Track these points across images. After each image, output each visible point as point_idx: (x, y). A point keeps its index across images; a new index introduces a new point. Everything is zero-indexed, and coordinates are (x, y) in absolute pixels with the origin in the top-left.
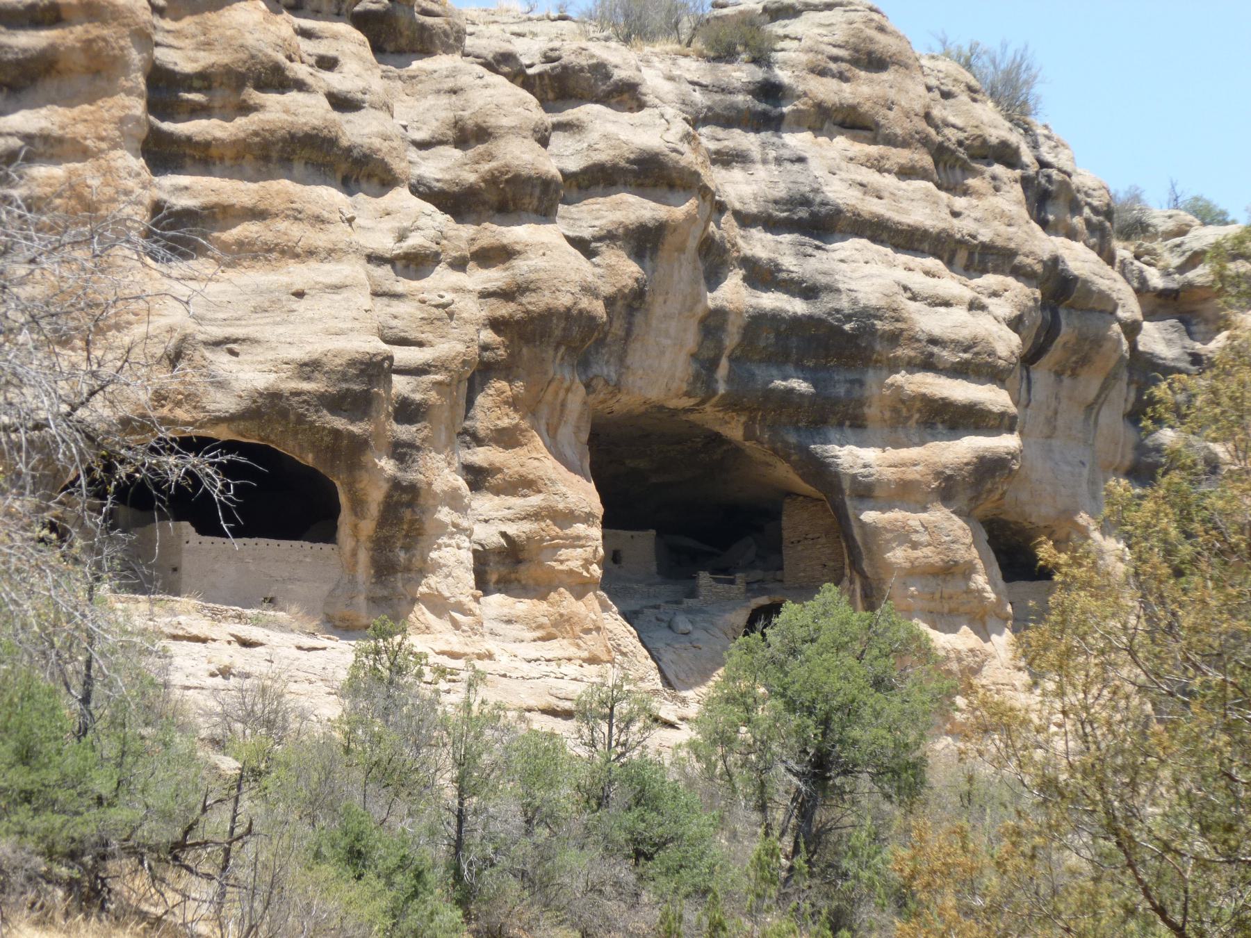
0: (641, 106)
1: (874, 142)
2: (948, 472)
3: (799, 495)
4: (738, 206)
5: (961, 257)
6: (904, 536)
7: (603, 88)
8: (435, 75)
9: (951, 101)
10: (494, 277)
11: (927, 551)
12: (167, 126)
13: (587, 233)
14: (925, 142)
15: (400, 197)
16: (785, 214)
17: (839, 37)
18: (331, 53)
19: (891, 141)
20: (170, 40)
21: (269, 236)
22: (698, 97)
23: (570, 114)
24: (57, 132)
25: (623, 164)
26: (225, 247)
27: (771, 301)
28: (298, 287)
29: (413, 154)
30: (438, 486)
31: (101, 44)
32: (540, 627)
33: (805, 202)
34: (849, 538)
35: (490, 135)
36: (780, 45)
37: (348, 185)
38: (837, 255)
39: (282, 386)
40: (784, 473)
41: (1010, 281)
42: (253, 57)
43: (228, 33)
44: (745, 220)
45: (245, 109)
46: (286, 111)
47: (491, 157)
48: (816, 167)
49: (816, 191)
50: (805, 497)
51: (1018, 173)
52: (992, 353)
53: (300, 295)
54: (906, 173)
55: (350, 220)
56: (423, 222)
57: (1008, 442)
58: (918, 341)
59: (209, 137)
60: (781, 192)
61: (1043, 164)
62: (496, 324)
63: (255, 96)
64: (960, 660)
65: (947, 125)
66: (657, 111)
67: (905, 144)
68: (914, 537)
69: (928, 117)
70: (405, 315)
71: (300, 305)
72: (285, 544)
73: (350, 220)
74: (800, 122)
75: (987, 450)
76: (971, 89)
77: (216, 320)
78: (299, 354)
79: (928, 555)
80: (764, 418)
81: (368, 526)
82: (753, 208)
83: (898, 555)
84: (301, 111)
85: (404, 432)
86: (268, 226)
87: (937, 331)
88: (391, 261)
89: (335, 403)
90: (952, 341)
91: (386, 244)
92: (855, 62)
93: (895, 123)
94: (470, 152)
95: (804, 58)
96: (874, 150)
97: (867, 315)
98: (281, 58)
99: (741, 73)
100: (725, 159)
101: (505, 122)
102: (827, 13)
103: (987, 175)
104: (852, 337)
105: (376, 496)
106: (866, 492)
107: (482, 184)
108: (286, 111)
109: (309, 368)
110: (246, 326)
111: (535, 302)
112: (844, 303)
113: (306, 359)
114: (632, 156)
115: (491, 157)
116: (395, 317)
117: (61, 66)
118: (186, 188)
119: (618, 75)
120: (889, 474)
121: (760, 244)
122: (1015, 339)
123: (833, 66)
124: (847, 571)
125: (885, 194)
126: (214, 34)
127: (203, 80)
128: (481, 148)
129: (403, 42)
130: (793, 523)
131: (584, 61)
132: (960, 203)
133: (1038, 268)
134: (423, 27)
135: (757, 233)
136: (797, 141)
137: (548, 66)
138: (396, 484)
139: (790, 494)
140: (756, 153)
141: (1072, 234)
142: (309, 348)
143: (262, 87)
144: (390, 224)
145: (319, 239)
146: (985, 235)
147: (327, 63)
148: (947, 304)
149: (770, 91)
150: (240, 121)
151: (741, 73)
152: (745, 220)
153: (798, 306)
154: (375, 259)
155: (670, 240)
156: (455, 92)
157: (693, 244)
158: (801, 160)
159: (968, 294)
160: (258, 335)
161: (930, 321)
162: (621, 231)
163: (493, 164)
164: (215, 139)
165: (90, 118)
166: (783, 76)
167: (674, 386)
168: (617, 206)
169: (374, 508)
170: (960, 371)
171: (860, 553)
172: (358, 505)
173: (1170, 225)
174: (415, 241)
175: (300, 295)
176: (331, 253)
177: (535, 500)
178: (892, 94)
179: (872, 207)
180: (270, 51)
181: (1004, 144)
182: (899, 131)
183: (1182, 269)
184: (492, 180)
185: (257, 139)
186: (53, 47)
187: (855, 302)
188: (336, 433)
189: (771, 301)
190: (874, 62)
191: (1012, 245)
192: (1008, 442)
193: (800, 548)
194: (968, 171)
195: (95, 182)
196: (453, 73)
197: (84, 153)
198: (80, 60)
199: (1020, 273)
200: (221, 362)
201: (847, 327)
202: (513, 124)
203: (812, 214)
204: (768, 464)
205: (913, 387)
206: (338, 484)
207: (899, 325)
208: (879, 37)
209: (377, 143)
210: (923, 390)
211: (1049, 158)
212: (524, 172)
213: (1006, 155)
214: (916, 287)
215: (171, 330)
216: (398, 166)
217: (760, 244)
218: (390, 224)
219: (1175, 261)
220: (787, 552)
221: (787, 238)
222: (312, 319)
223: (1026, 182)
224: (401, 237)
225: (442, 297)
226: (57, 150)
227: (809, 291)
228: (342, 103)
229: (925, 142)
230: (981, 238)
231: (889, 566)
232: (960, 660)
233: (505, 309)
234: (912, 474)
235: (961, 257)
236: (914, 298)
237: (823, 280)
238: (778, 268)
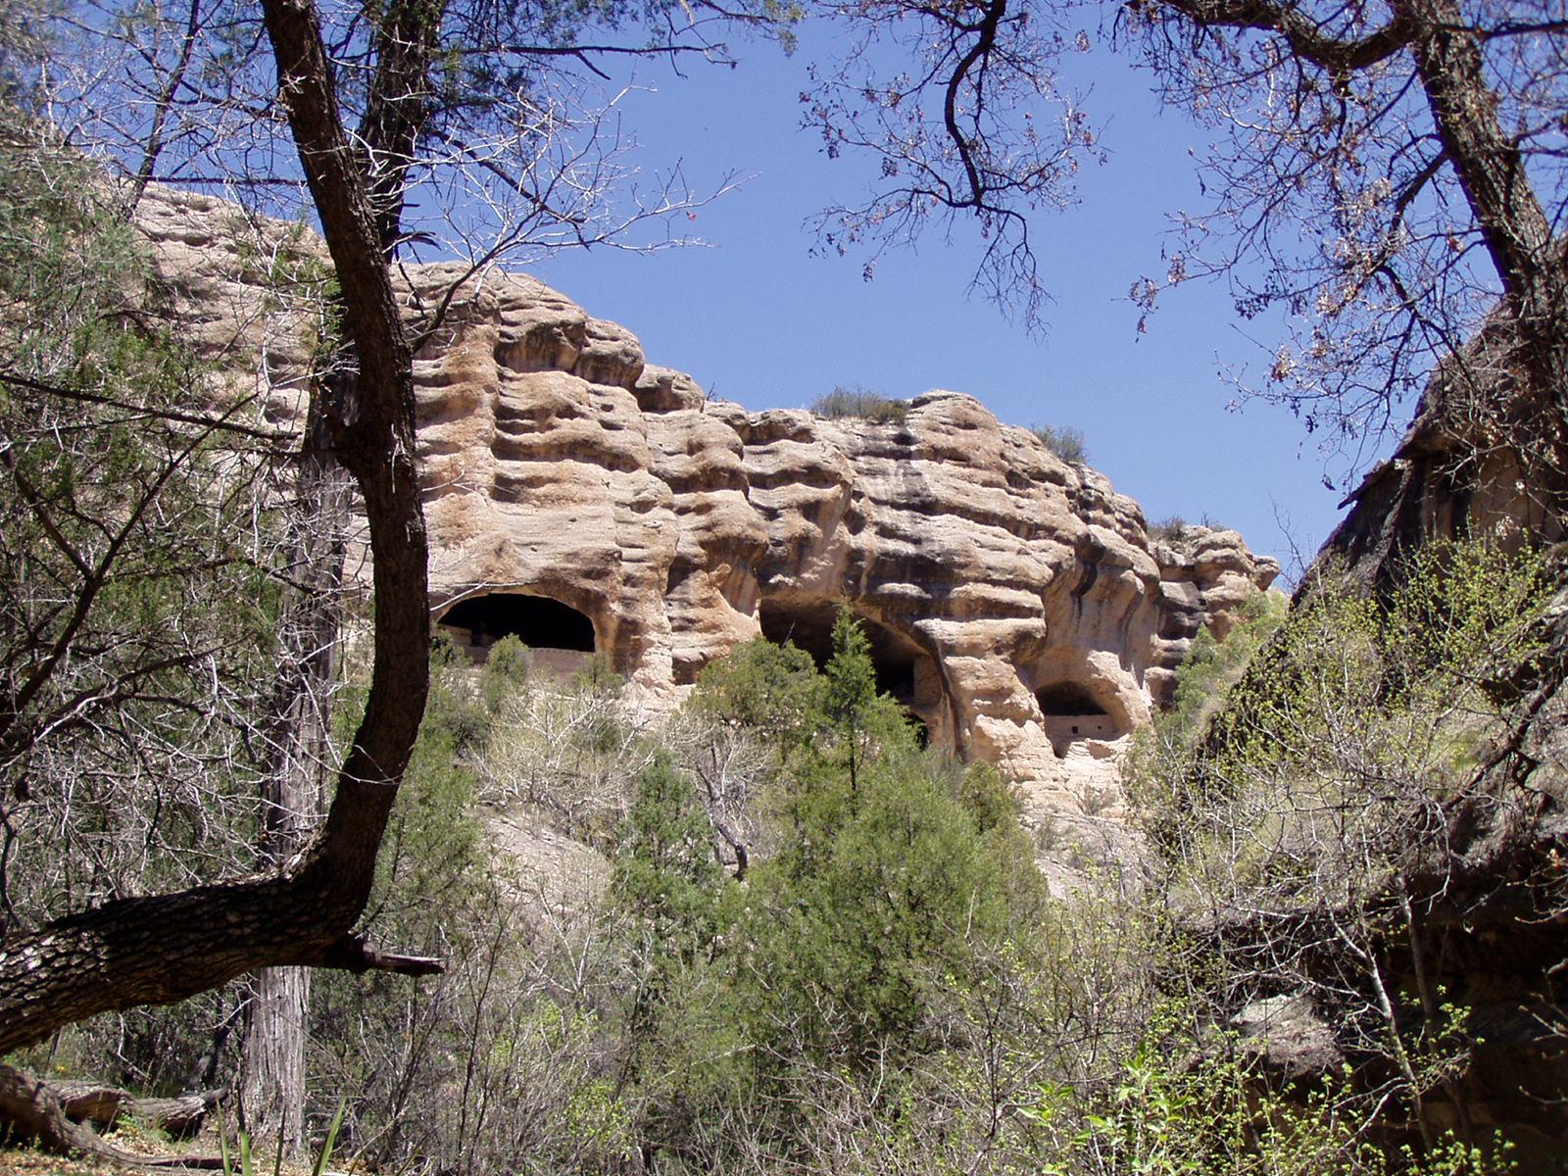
0: (812, 440)
1: (969, 466)
4: (873, 495)
5: (1024, 530)
6: (973, 672)
7: (791, 431)
10: (702, 520)
11: (986, 681)
12: (508, 436)
13: (776, 506)
14: (1001, 468)
15: (642, 475)
19: (978, 467)
20: (515, 394)
21: (561, 492)
22: (860, 442)
23: (773, 445)
24: (446, 439)
26: (538, 498)
27: (892, 545)
29: (664, 458)
30: (649, 622)
33: (917, 495)
34: (943, 676)
37: (611, 467)
40: (908, 641)
41: (1053, 543)
44: (877, 502)
45: (551, 427)
47: (704, 458)
48: (927, 477)
51: (1064, 488)
52: (1026, 575)
53: (573, 520)
54: (986, 484)
57: (1037, 623)
60: (903, 489)
61: (1084, 487)
62: (702, 544)
63: (557, 421)
64: (1005, 741)
65: (1016, 460)
67: (986, 468)
69: (1002, 456)
70: (634, 533)
72: (564, 651)
73: (608, 484)
74: (920, 455)
76: (1034, 443)
78: (567, 550)
79: (986, 684)
81: (610, 642)
82: (884, 498)
83: (968, 683)
85: (628, 591)
87: (992, 563)
88: (631, 505)
89: (588, 575)
91: (630, 497)
92: (958, 425)
93: (980, 457)
95: (924, 422)
96: (967, 471)
97: (950, 553)
98: (573, 402)
99: (890, 430)
100: (872, 473)
101: (712, 440)
104: (941, 566)
105: (612, 626)
106: (951, 649)
109: (572, 556)
111: (720, 531)
112: (936, 548)
115: (704, 458)
117: (450, 405)
119: (799, 424)
120: (964, 640)
121: (888, 516)
122: (1051, 572)
123: (943, 427)
127: (530, 414)
129: (667, 404)
130: (920, 670)
132: (1024, 502)
133: (1073, 538)
134: (675, 395)
135: (886, 509)
136: (916, 464)
138: (623, 620)
139: (919, 655)
140: (891, 471)
141: (1106, 525)
143: (561, 415)
144: (632, 487)
145: (588, 493)
146: (1038, 520)
147: (607, 408)
148: (1002, 550)
149: (904, 439)
150: (548, 433)
151: (890, 430)
152: (877, 502)
153: (910, 549)
154: (621, 504)
155: (824, 510)
157: (838, 512)
158: (919, 474)
159: (1018, 546)
161: (987, 558)
166: (912, 432)
167: (832, 588)
168: (794, 491)
169: (612, 633)
170: (1009, 584)
172: (603, 631)
173: (1195, 533)
175: (573, 520)
176: (596, 500)
177: (719, 635)
178: (979, 443)
179: (961, 499)
181: (1054, 473)
183: (1196, 555)
184: (703, 470)
186: (445, 396)
187: (942, 546)
188: (587, 591)
189: (892, 545)
190: (971, 426)
192: (1037, 623)
194: (1029, 485)
196: (691, 417)
197: (458, 449)
198: (459, 402)
199: (1058, 539)
200: (527, 555)
201: (938, 560)
203: (922, 502)
208: (972, 412)
209: (628, 446)
211: (1088, 482)
212: (720, 465)
213: (1057, 479)
214: (983, 541)
215: (497, 537)
216: (640, 458)
217: (888, 516)
218: (632, 487)
219: (1194, 550)
220: (917, 687)
221: (905, 513)
223: (1070, 495)
226: (447, 448)
227: (917, 542)
228: (609, 426)
229: (1001, 468)
231: (964, 689)
232: (1005, 741)
233: (707, 536)
234: (977, 639)
235: (1024, 530)
236: (982, 546)
237: (924, 535)
238: (898, 529)
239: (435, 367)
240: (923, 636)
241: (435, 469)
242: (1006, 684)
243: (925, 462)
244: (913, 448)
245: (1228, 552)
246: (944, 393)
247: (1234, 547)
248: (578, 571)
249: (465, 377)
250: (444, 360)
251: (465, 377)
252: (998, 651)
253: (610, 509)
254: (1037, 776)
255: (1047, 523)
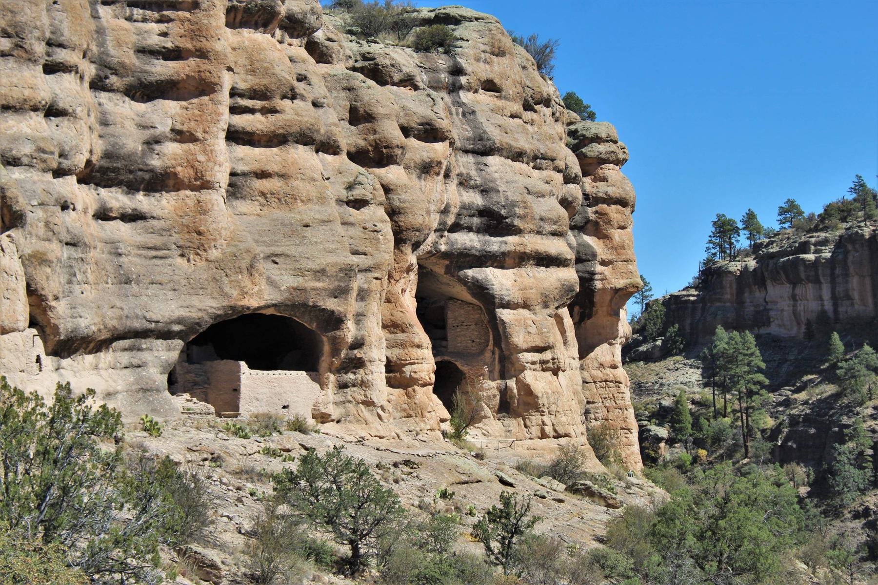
2: (547, 293)
3: (459, 300)
7: (397, 77)
8: (336, 77)
9: (525, 71)
16: (472, 146)
17: (485, 40)
18: (303, 72)
19: (506, 98)
25: (413, 125)
26: (263, 194)
28: (305, 222)
31: (208, 74)
32: (404, 410)
35: (374, 118)
36: (459, 43)
38: (493, 169)
39: (306, 285)
42: (280, 81)
43: (265, 65)
45: (273, 111)
46: (297, 114)
47: (375, 132)
49: (485, 132)
50: (462, 301)
55: (328, 179)
56: (361, 179)
58: (535, 219)
59: (255, 129)
60: (470, 134)
66: (425, 93)
68: (529, 329)
71: (308, 232)
75: (565, 280)
77: (264, 242)
80: (457, 262)
84: (304, 113)
86: (287, 183)
87: (543, 214)
90: (549, 219)
94: (361, 126)
96: (500, 103)
102: (475, 23)
103: (542, 114)
107: (370, 148)
108: (297, 114)
109: (321, 273)
110: (281, 246)
113: (318, 268)
114: (418, 121)
116: (352, 238)
117: (180, 85)
118: (242, 159)
119: (405, 70)
123: (483, 55)
124: (490, 347)
125: (508, 131)
126: (257, 65)
128: (368, 125)
131: (388, 62)
137: (367, 63)
142: (318, 261)
148: (543, 196)
150: (272, 118)
156: (349, 90)
158: (474, 112)
160: (289, 252)
162: (412, 165)
163: (377, 136)
164: (258, 129)
165: (199, 119)
171: (501, 338)
174: (358, 193)
175: (307, 226)
176: (322, 199)
180: (287, 77)
182: (511, 93)
185: (281, 131)
191: (555, 155)
193: (458, 330)
195: (202, 158)
202: (387, 113)
204: (448, 284)
205: (532, 246)
206: (325, 339)
207: (526, 211)
210: (537, 247)
222: (316, 242)
224: (350, 187)
225: (375, 226)
230: (542, 152)
236: (529, 193)
239: (164, 34)
240: (481, 291)
241: (168, 163)
242: (551, 340)
243: (470, 95)
244: (463, 80)
245: (612, 147)
246: (475, 14)
247: (615, 142)
248: (325, 290)
249: (202, 54)
250: (174, 28)
251: (202, 54)
252: (546, 306)
253: (334, 210)
254: (573, 434)
255: (549, 154)
